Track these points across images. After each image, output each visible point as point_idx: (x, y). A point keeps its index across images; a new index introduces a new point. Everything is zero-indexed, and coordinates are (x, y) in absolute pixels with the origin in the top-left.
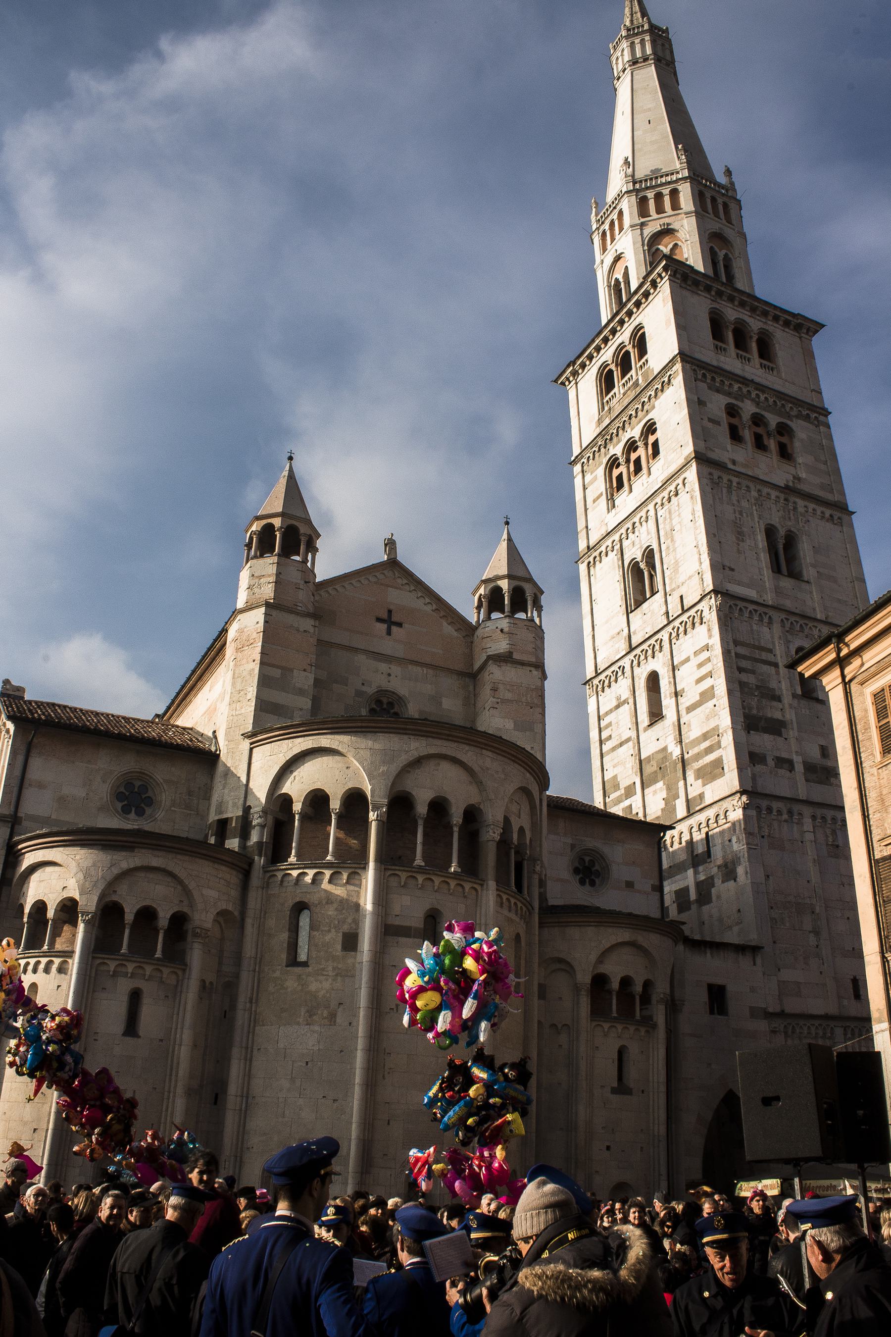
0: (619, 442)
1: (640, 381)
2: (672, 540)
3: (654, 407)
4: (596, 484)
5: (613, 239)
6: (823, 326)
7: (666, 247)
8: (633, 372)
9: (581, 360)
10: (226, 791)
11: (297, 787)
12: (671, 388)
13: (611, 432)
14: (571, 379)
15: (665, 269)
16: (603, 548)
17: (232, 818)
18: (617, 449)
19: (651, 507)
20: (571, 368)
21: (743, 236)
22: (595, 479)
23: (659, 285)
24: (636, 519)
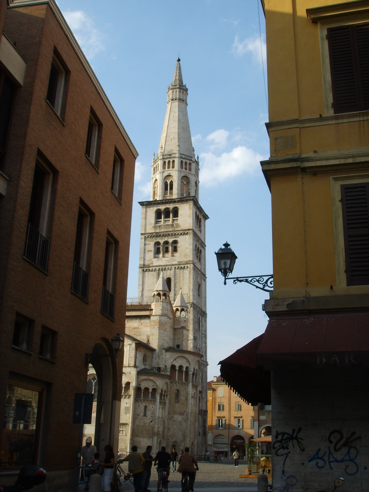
0: (162, 239)
1: (174, 226)
3: (178, 237)
5: (169, 168)
6: (209, 218)
7: (185, 182)
8: (171, 219)
10: (159, 361)
11: (177, 365)
15: (193, 199)
16: (151, 269)
17: (162, 368)
18: (162, 241)
19: (173, 267)
21: (199, 182)
22: (150, 244)
24: (167, 267)
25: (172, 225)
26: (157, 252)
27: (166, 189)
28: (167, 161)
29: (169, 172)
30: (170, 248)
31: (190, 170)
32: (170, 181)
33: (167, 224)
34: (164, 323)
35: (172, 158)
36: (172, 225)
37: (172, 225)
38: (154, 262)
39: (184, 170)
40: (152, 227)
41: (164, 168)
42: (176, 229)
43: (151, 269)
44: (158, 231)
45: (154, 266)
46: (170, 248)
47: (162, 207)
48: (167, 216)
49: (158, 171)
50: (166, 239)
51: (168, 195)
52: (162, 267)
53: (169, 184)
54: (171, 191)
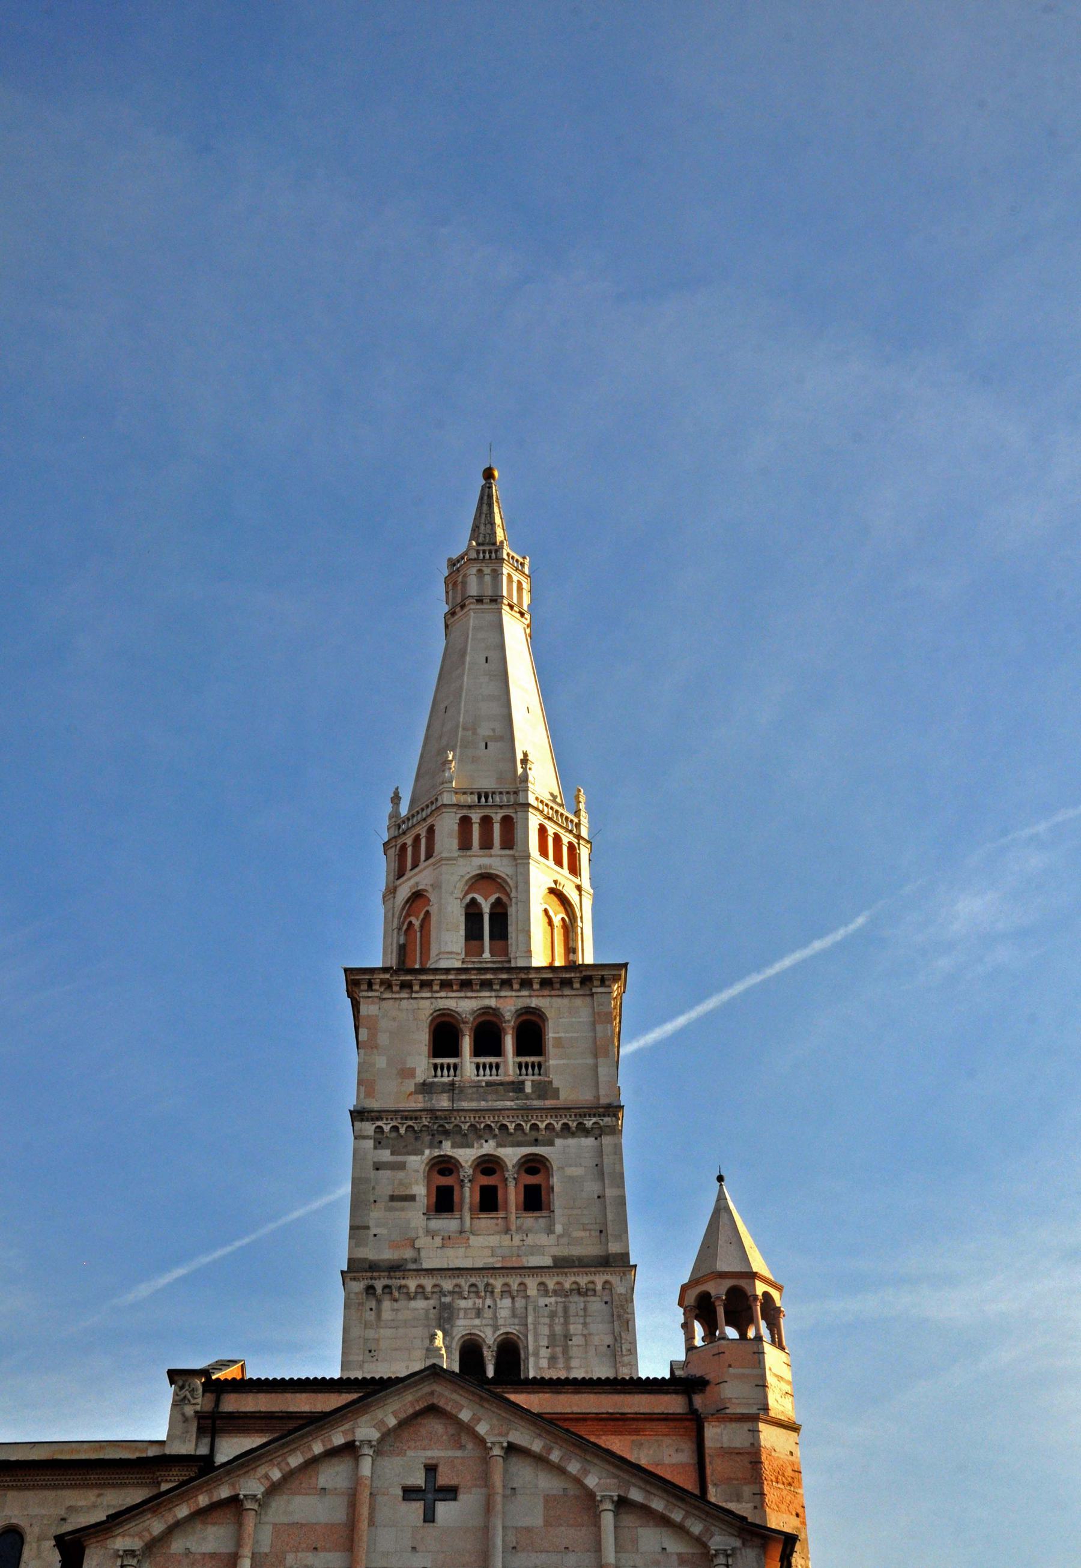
0: (470, 1146)
1: (528, 1089)
2: (566, 1350)
3: (551, 1143)
4: (401, 1174)
9: (409, 978)
12: (590, 1141)
13: (457, 1122)
14: (376, 987)
16: (412, 1284)
18: (466, 1156)
19: (532, 1284)
20: (387, 976)
22: (402, 1166)
23: (594, 990)
24: (498, 1283)
25: (517, 1087)
26: (444, 1202)
27: (473, 932)
28: (476, 817)
29: (486, 861)
30: (512, 1195)
31: (574, 870)
32: (492, 899)
33: (488, 1078)
34: (789, 1469)
35: (501, 807)
36: (517, 1087)
37: (513, 1083)
38: (423, 1254)
39: (551, 862)
40: (412, 1088)
41: (465, 845)
42: (537, 1103)
43: (412, 1284)
44: (443, 1102)
45: (430, 1271)
46: (512, 1195)
47: (465, 1006)
48: (488, 1041)
49: (429, 855)
50: (488, 1147)
51: (487, 955)
52: (473, 1280)
53: (486, 909)
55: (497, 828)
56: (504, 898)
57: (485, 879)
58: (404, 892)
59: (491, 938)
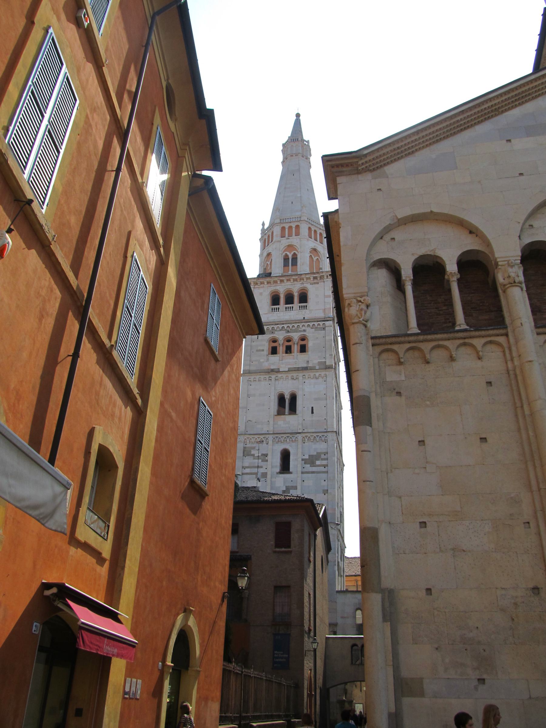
26: (274, 351)
27: (286, 264)
28: (287, 226)
30: (296, 348)
32: (292, 253)
39: (313, 240)
41: (283, 236)
46: (296, 348)
47: (282, 289)
48: (289, 299)
49: (272, 241)
51: (290, 272)
53: (290, 256)
54: (294, 267)
55: (294, 229)
56: (297, 253)
57: (290, 247)
58: (265, 254)
59: (292, 265)
